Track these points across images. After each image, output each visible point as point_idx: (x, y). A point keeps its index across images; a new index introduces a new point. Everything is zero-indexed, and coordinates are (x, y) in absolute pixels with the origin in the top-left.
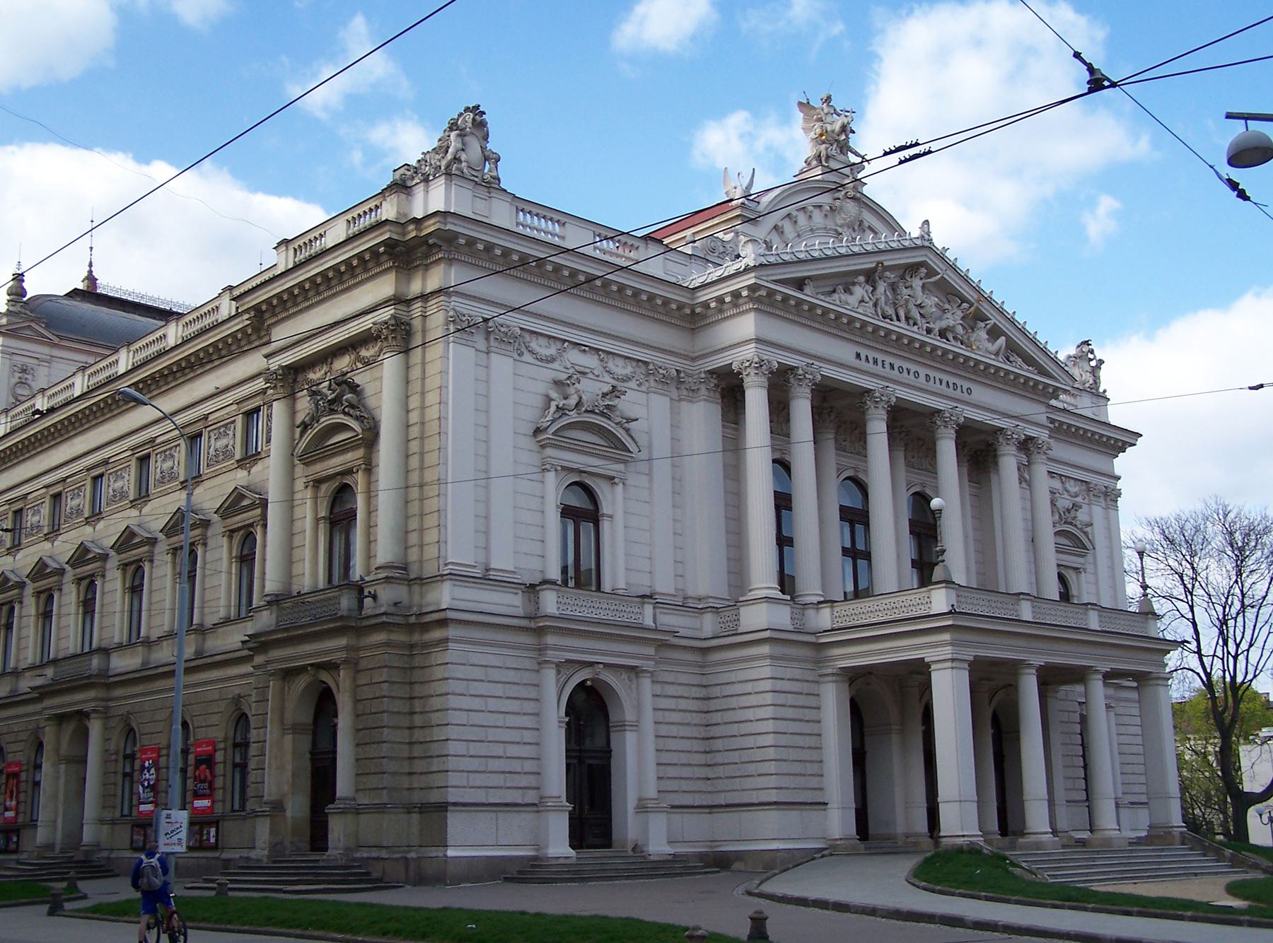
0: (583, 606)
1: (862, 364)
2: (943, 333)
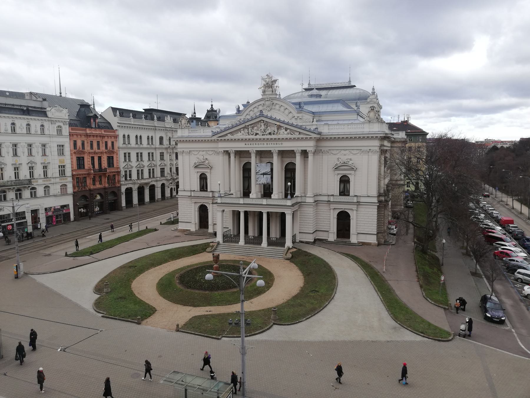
0: (203, 194)
1: (247, 146)
2: (270, 134)
